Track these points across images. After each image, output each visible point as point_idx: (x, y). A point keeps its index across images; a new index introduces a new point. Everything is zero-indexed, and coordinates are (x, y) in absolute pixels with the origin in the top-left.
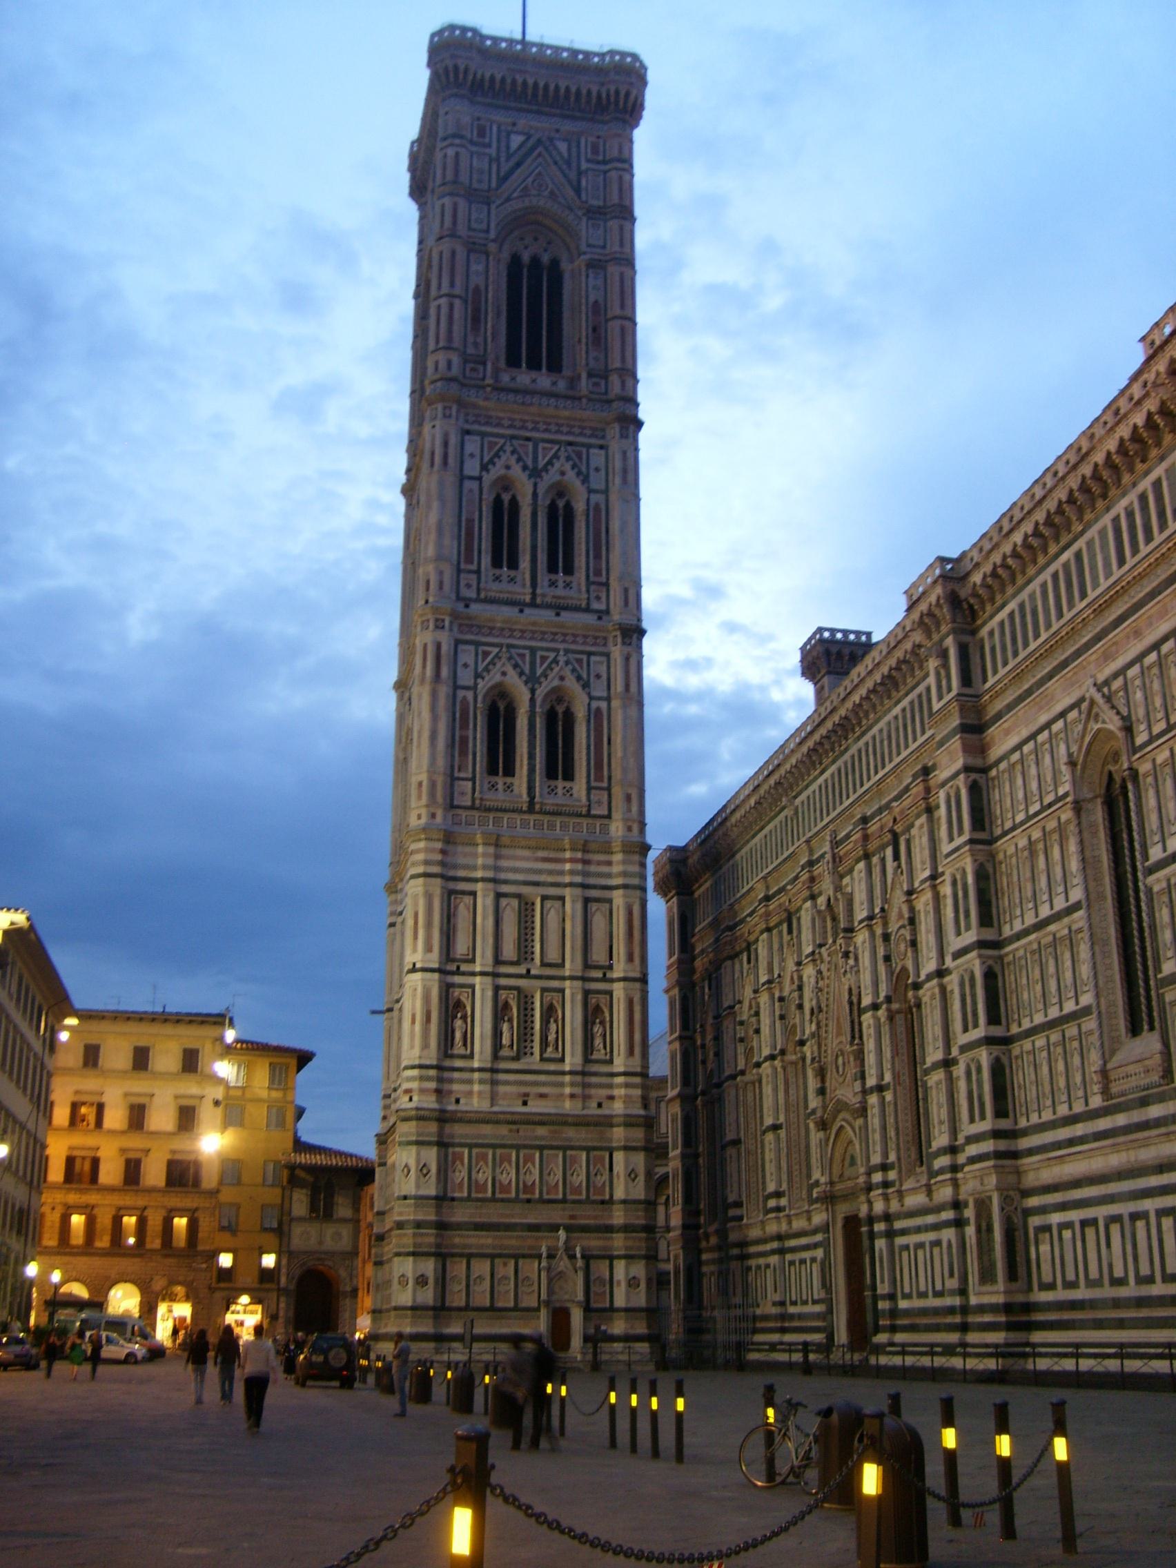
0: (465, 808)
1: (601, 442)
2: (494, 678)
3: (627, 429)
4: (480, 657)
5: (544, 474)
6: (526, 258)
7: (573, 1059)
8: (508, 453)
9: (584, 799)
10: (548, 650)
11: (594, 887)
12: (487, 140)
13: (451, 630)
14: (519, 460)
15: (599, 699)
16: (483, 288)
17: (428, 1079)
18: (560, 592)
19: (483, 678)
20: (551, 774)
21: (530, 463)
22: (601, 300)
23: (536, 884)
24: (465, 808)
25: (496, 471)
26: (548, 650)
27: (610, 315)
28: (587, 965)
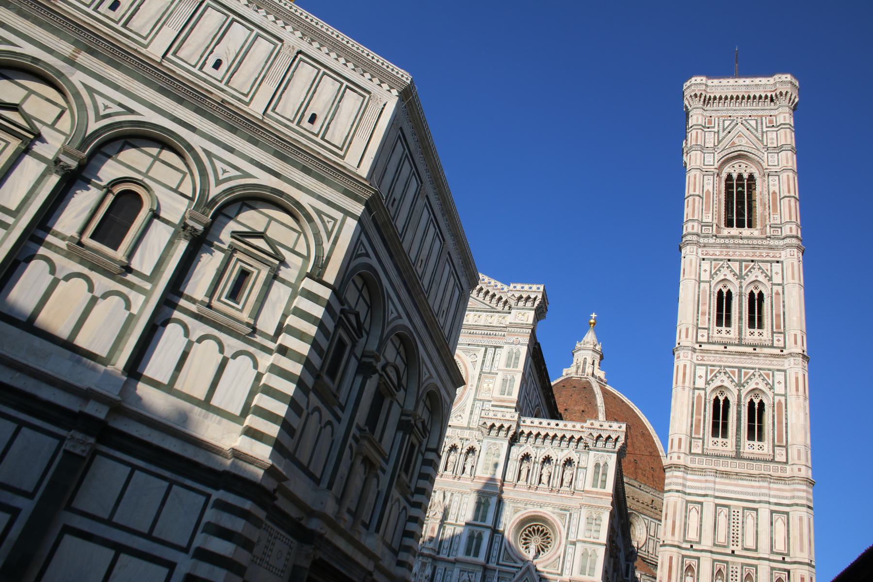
2: (717, 383)
4: (709, 372)
5: (745, 277)
6: (735, 176)
8: (725, 268)
9: (771, 452)
10: (748, 368)
12: (713, 125)
13: (692, 358)
19: (709, 384)
20: (751, 437)
21: (738, 272)
22: (777, 191)
24: (698, 454)
26: (748, 368)
27: (781, 197)
28: (772, 552)
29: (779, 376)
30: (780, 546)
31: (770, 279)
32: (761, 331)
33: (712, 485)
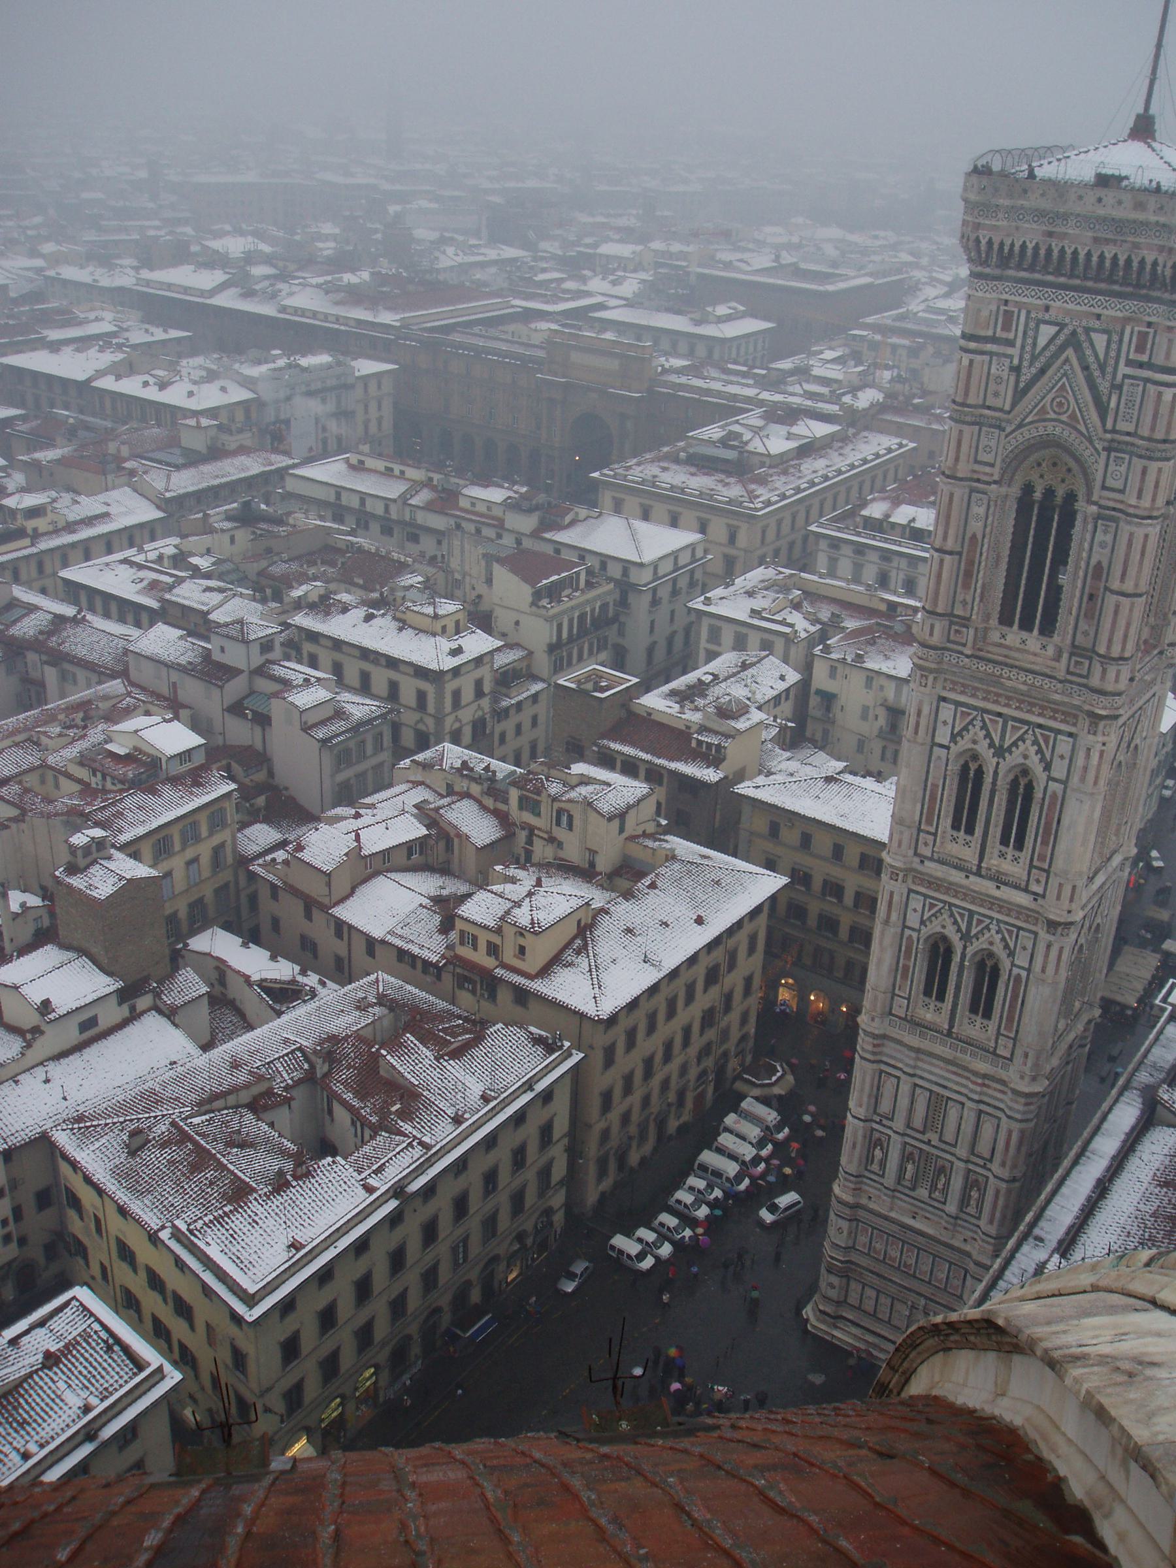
0: (900, 1018)
1: (1073, 730)
2: (934, 927)
3: (1097, 725)
4: (927, 908)
5: (1007, 755)
7: (951, 1208)
8: (978, 728)
11: (989, 1105)
12: (1011, 336)
14: (985, 737)
15: (1019, 967)
16: (979, 537)
17: (851, 1181)
18: (1007, 866)
22: (1105, 564)
23: (945, 1087)
24: (900, 1018)
25: (964, 744)
29: (1026, 939)
30: (984, 1148)
31: (1048, 767)
32: (1017, 854)
33: (912, 1062)
